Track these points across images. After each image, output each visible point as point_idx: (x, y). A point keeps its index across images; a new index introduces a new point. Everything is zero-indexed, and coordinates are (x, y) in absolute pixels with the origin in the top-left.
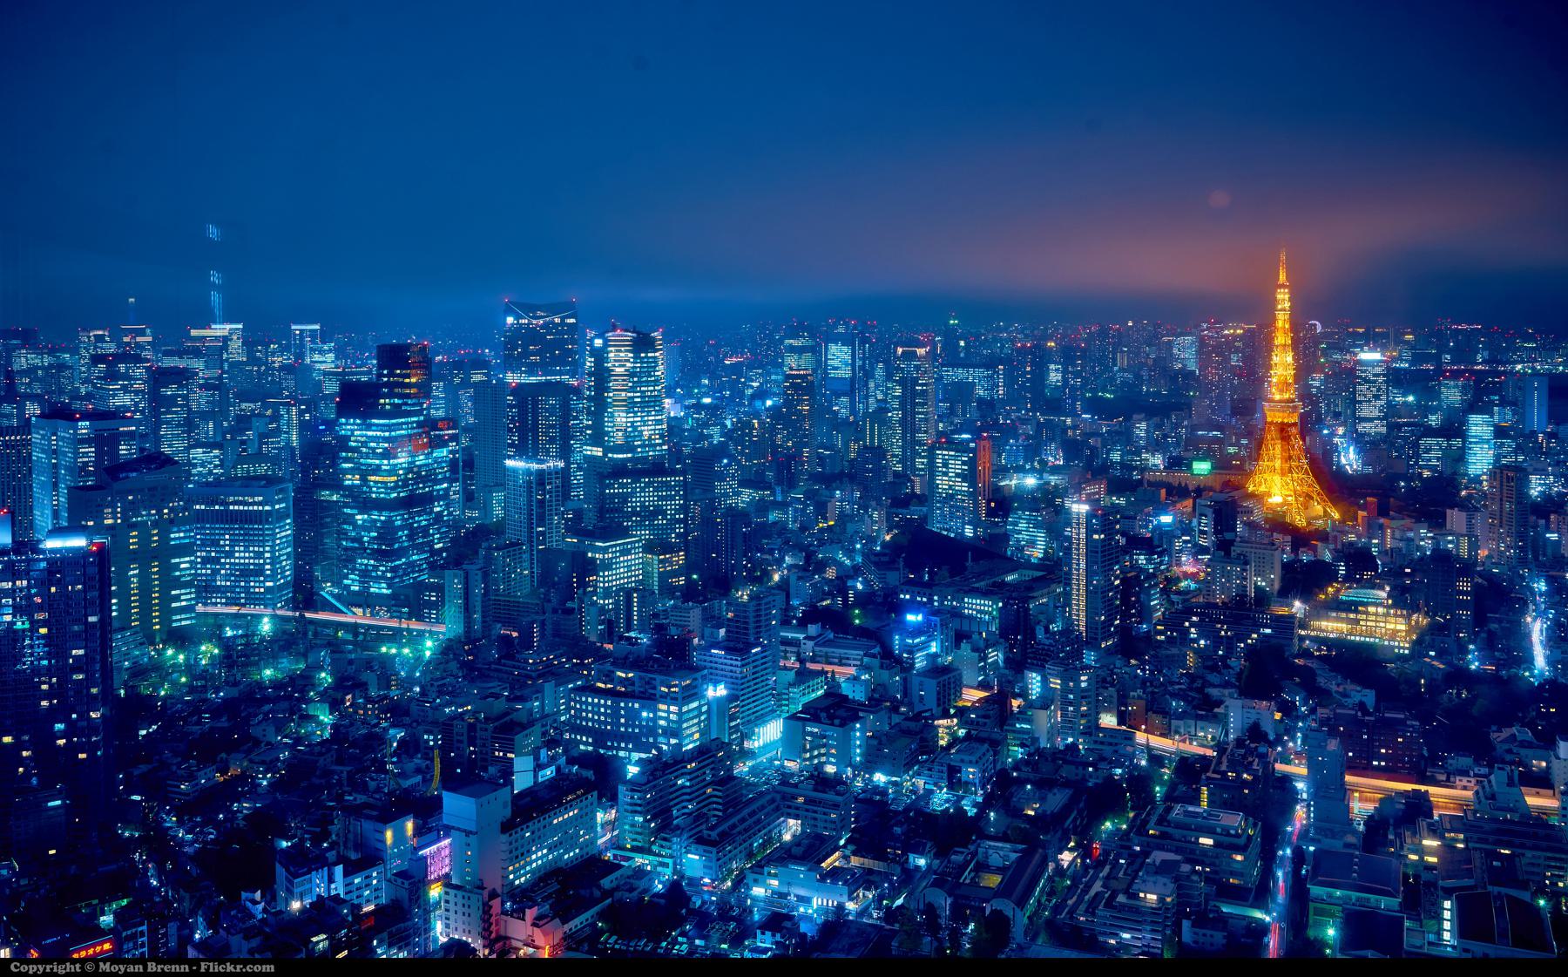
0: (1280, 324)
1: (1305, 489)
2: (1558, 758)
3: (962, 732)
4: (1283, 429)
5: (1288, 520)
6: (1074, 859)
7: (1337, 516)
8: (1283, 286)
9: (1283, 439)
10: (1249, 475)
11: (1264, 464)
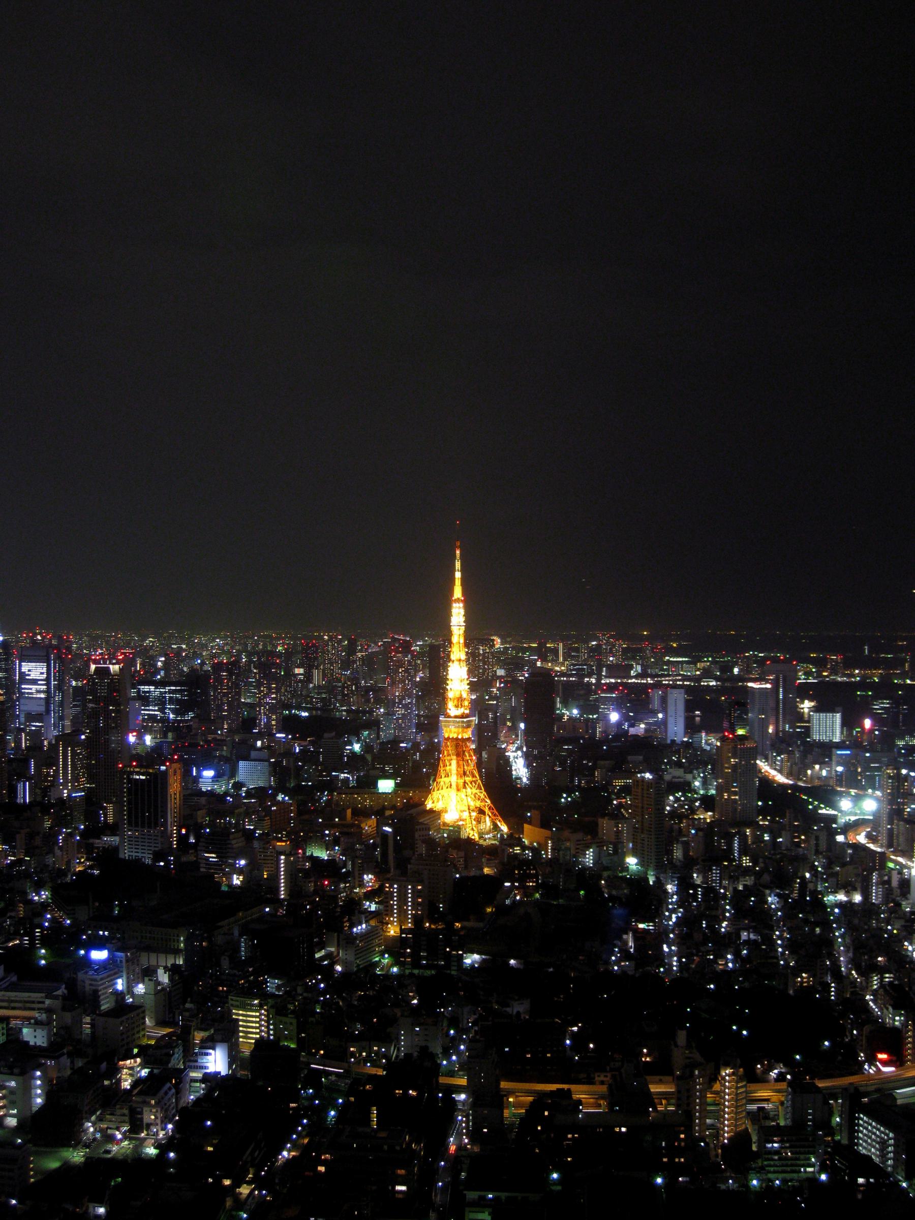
0: (455, 639)
1: (478, 804)
2: (676, 1046)
3: (144, 1072)
4: (459, 744)
5: (464, 835)
6: (252, 1191)
7: (505, 828)
8: (458, 600)
9: (458, 755)
10: (427, 791)
11: (443, 780)
